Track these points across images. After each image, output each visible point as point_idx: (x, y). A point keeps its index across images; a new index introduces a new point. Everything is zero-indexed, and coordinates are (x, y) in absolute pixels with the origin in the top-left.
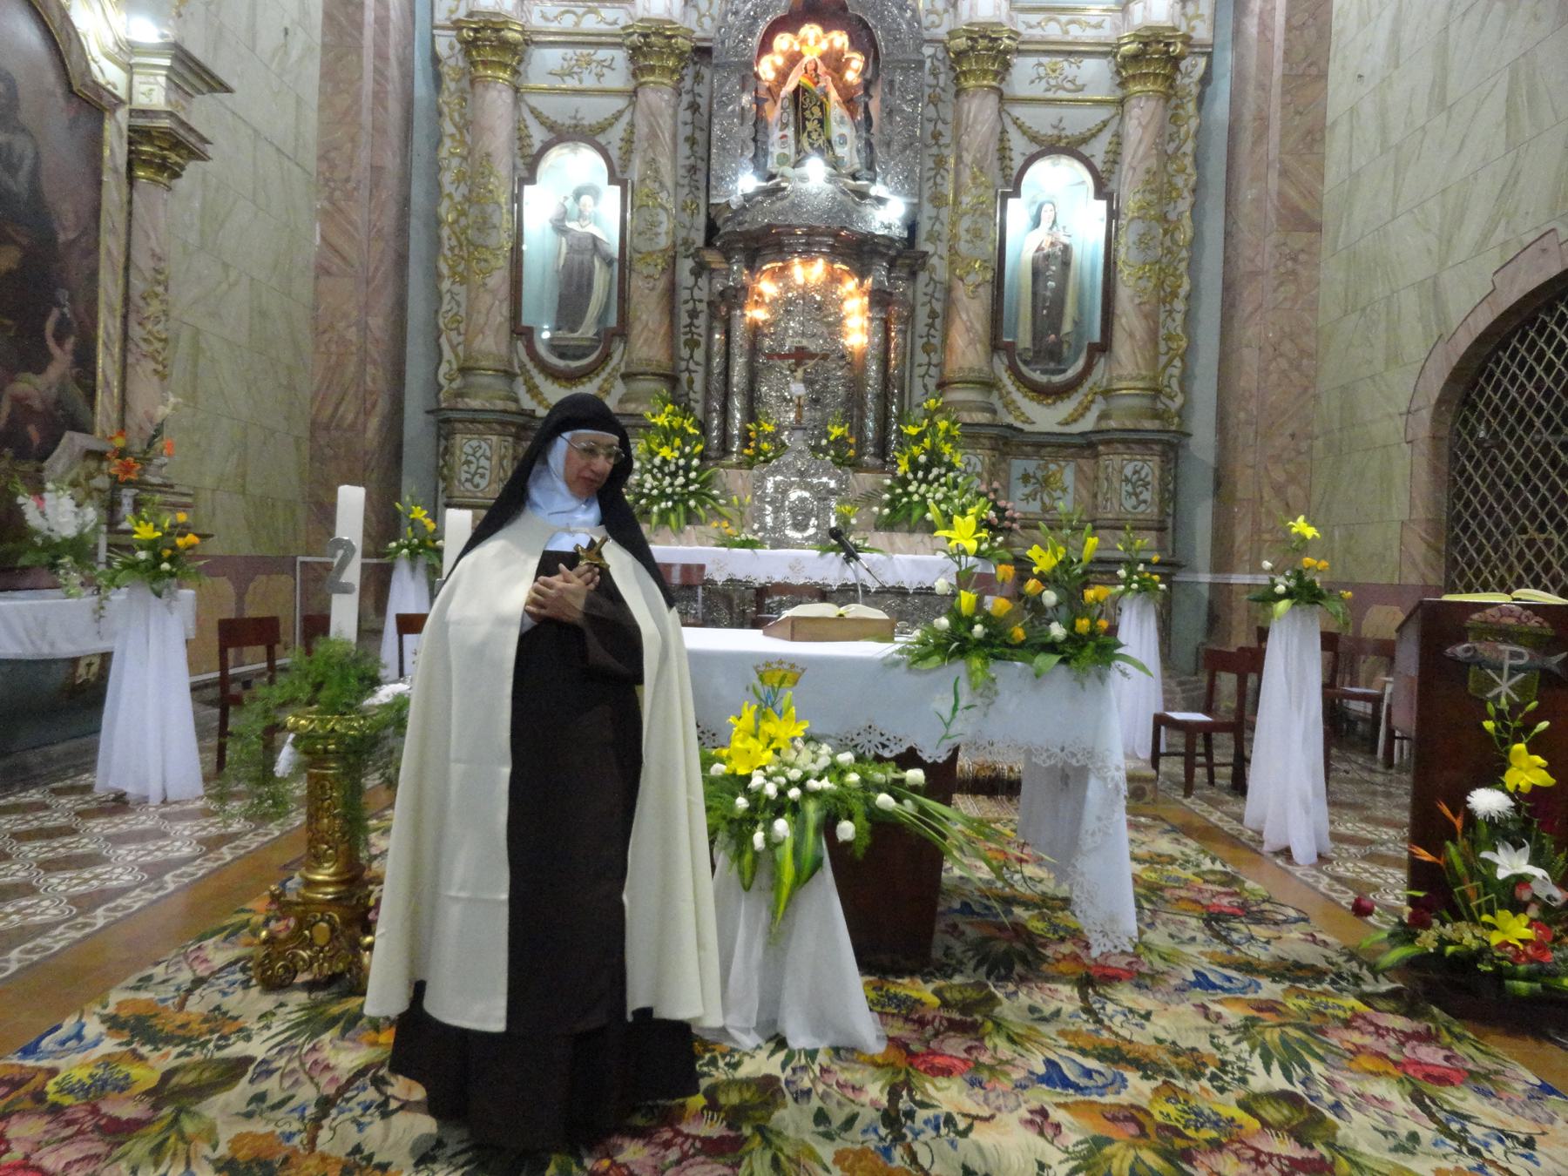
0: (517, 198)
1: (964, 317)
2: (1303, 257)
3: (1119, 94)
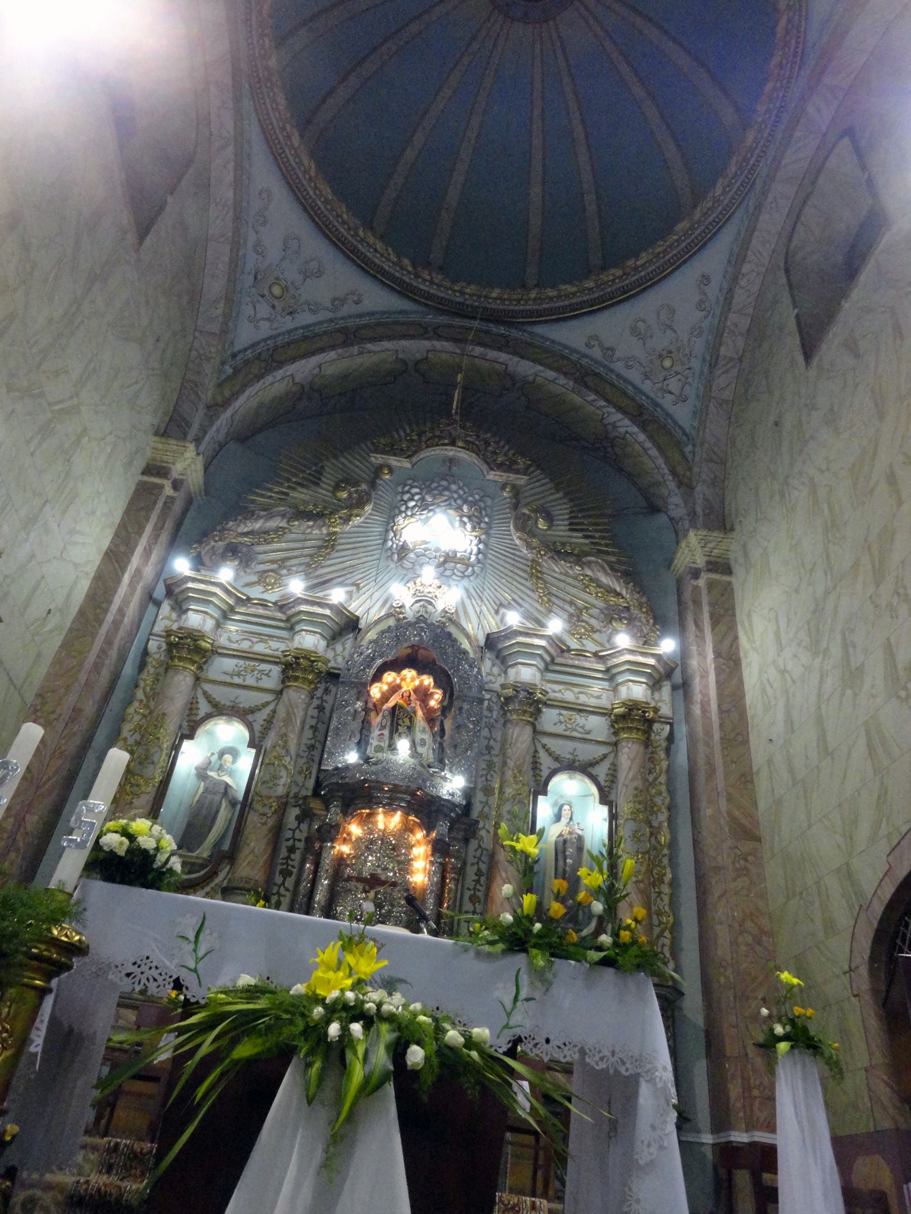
0: (176, 748)
1: (504, 875)
3: (614, 739)
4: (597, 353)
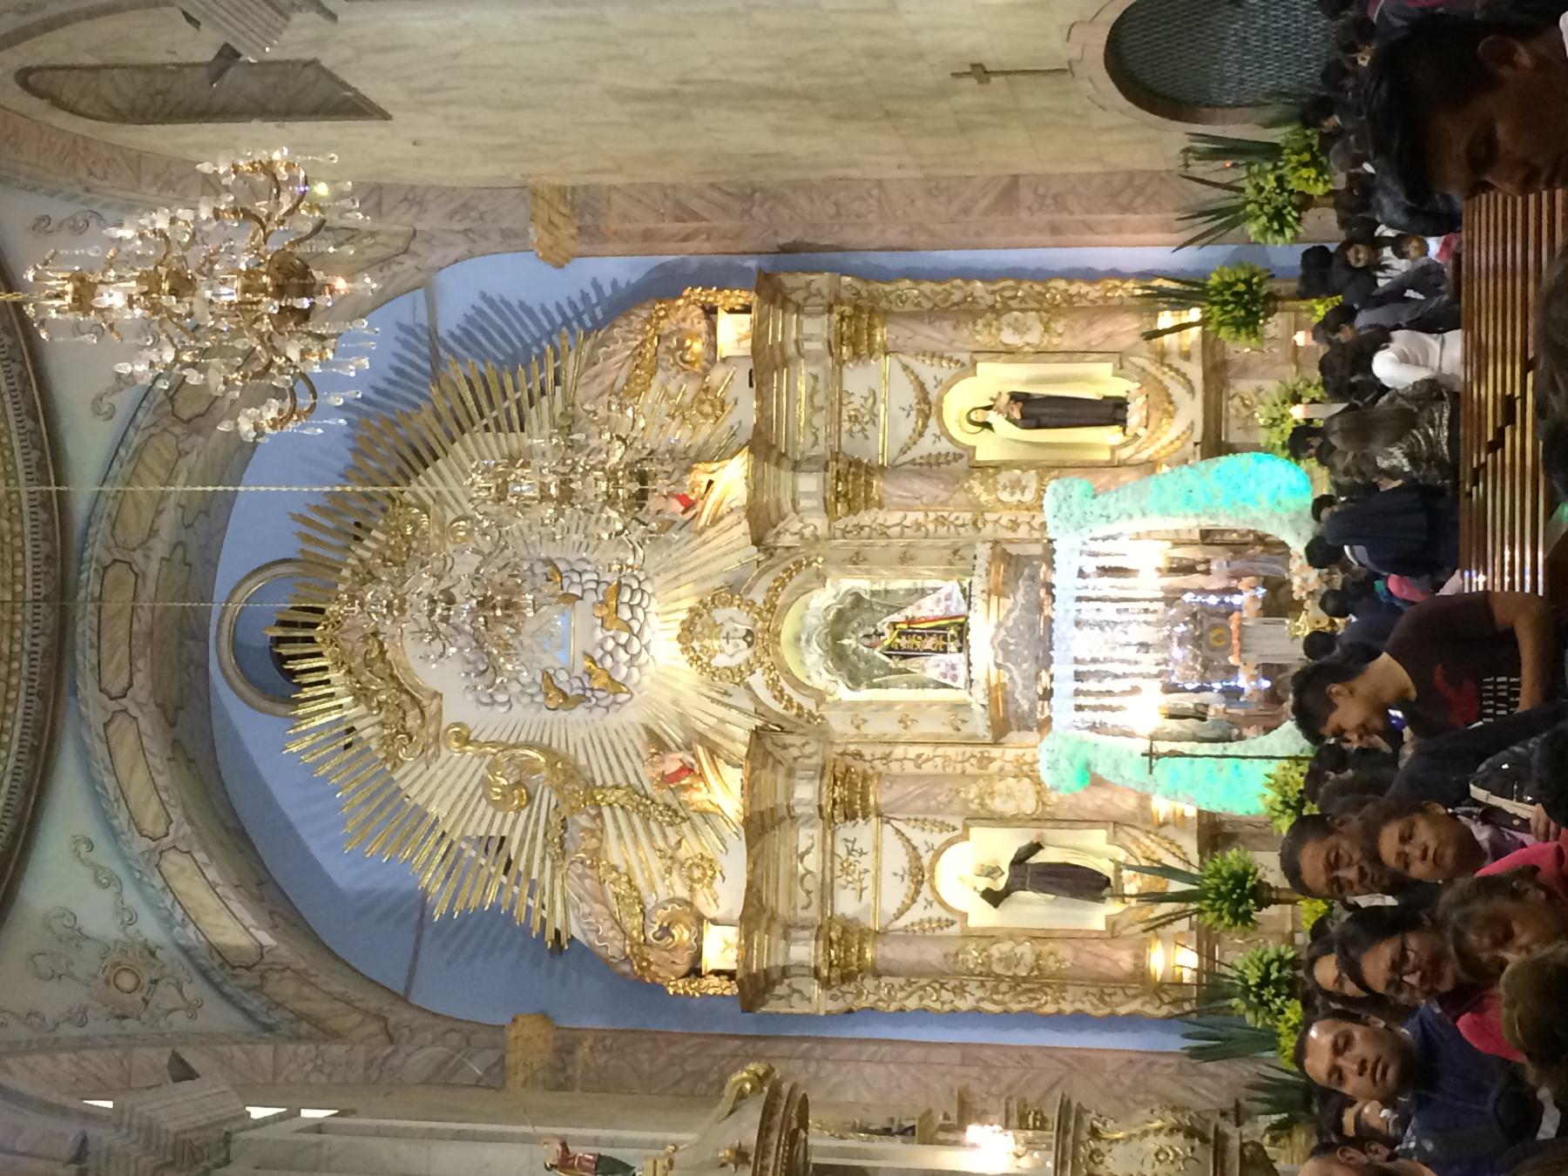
2: (1041, 190)
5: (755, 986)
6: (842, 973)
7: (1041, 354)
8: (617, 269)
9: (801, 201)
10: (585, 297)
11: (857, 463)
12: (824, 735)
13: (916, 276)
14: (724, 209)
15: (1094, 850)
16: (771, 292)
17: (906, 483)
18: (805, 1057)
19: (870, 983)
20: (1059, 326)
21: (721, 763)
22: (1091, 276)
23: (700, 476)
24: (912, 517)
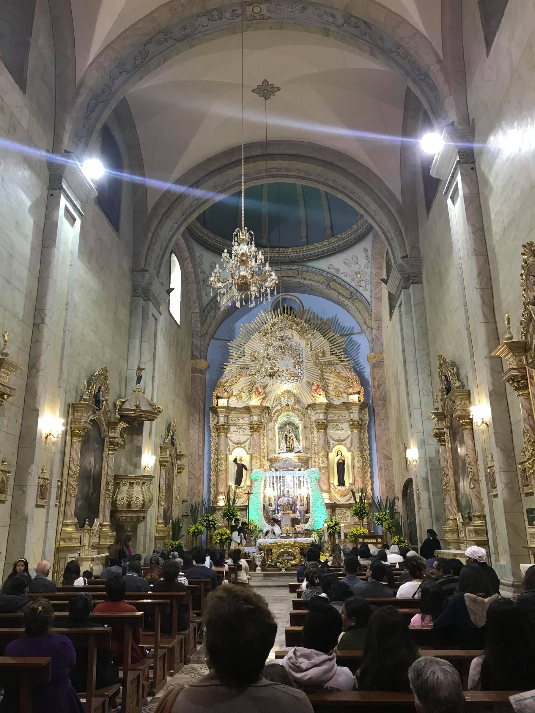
4: (332, 271)
5: (214, 410)
6: (218, 429)
7: (353, 467)
8: (367, 373)
9: (384, 411)
10: (361, 366)
11: (327, 426)
12: (268, 422)
13: (370, 438)
14: (381, 394)
15: (245, 483)
16: (363, 406)
17: (323, 437)
18: (200, 421)
19: (216, 435)
20: (359, 470)
21: (261, 400)
22: (372, 477)
23: (322, 392)
24: (316, 439)
